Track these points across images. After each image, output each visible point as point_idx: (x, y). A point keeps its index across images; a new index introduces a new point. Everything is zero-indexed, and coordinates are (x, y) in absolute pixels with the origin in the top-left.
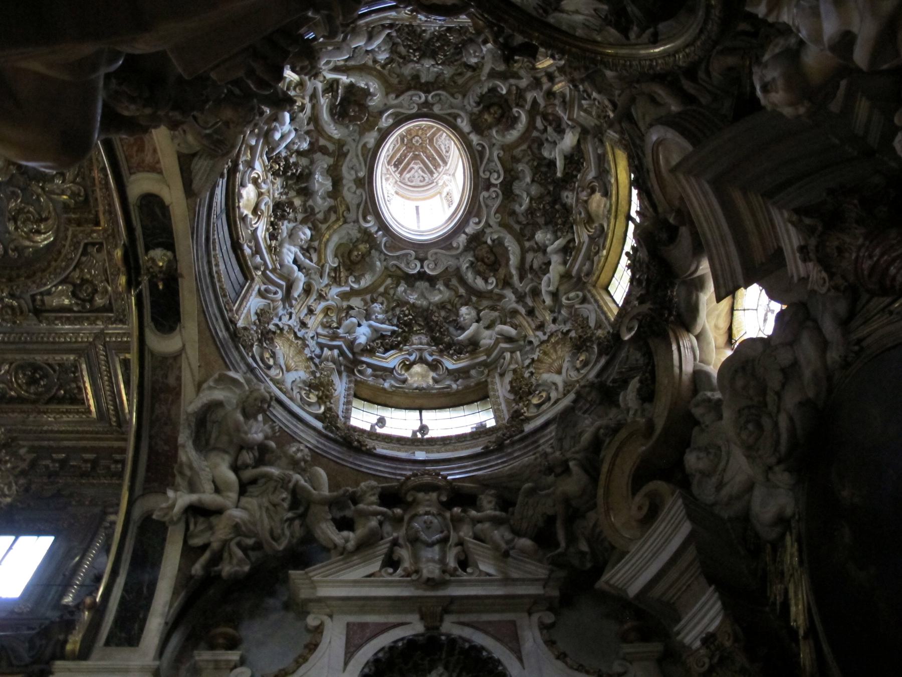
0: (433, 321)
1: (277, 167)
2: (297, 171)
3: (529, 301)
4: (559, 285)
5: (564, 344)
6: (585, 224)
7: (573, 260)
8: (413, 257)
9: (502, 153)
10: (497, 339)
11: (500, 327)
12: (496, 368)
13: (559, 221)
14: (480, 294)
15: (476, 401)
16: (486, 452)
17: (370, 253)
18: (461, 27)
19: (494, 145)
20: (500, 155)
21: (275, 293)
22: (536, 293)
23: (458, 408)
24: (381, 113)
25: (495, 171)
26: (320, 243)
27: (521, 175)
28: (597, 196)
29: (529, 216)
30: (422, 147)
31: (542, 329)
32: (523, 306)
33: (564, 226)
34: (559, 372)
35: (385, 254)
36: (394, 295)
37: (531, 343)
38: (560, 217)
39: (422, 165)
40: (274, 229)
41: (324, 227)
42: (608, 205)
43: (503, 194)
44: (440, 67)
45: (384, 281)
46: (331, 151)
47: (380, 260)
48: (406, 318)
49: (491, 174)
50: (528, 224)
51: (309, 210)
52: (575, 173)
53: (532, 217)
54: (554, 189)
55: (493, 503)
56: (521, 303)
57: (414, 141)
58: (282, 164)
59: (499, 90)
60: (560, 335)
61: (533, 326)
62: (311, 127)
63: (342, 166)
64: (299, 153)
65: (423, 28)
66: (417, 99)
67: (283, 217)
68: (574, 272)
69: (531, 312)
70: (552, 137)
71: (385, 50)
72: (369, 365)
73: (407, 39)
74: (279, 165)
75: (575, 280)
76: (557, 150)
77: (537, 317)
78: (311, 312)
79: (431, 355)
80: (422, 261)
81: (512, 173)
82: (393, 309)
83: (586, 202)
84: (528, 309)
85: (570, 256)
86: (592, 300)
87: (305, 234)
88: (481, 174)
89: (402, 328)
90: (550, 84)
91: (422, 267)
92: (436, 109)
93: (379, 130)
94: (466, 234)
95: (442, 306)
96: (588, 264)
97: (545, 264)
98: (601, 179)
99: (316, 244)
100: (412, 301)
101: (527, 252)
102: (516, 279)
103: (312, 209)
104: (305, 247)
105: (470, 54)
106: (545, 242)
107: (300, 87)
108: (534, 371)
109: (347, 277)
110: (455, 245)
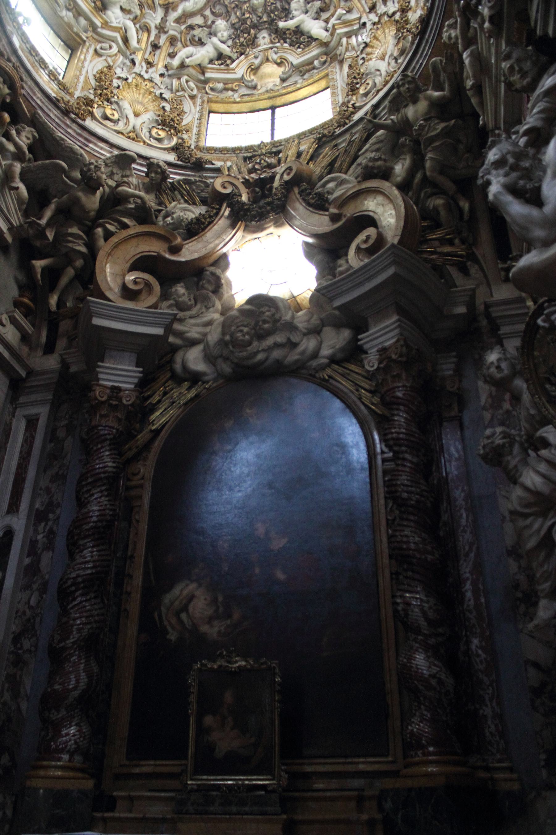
3: (163, 39)
4: (192, 66)
5: (154, 101)
6: (250, 67)
7: (217, 69)
10: (121, 28)
11: (130, 24)
12: (100, 42)
13: (242, 40)
15: (62, 40)
16: (54, 102)
22: (173, 41)
28: (279, 71)
29: (233, 5)
31: (149, 66)
32: (156, 35)
33: (240, 46)
34: (137, 115)
37: (133, 62)
38: (245, 38)
42: (277, 88)
50: (226, 6)
52: (288, 40)
53: (234, 8)
54: (266, 22)
55: (29, 142)
56: (157, 31)
60: (158, 93)
61: (146, 56)
68: (208, 75)
69: (155, 47)
70: (311, 7)
75: (203, 78)
76: (303, 17)
77: (154, 55)
83: (268, 60)
84: (156, 42)
85: (219, 65)
86: (198, 108)
96: (220, 86)
97: (200, 39)
98: (293, 71)
101: (202, 15)
102: (174, 15)
106: (218, 32)
108: (121, 88)
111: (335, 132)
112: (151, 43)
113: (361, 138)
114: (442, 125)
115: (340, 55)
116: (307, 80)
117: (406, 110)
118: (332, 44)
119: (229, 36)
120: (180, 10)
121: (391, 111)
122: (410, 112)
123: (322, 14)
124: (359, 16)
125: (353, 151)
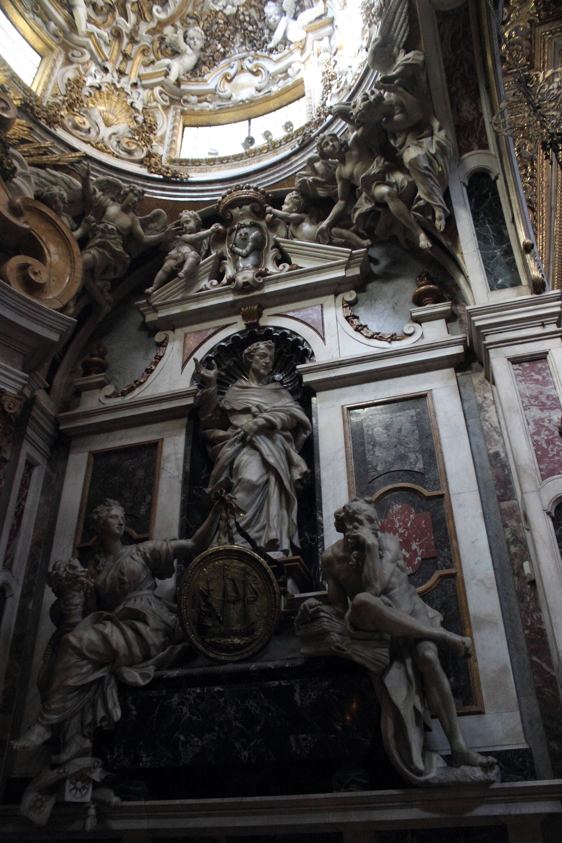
18: (215, 65)
44: (218, 9)
59: (160, 9)
65: (244, 48)
71: (270, 18)
73: (254, 33)
90: (123, 48)
105: (198, 39)
111: (40, 119)
113: (58, 161)
114: (120, 249)
115: (73, 55)
116: (36, 24)
117: (111, 202)
118: (75, 37)
121: (99, 183)
122: (113, 209)
123: (91, 7)
124: (108, 57)
125: (45, 158)
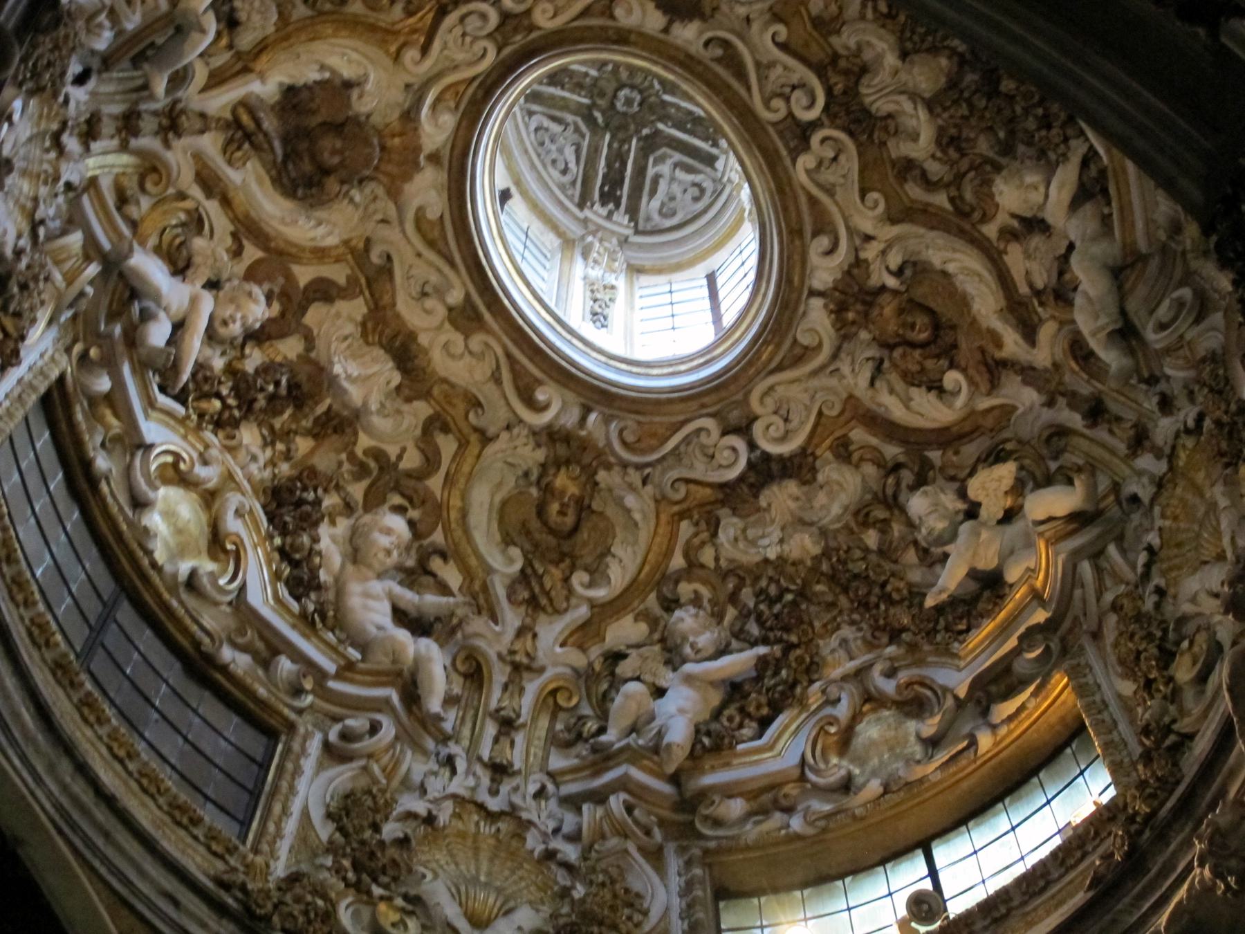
0: (856, 576)
1: (217, 404)
2: (277, 384)
8: (715, 433)
9: (782, 30)
14: (947, 438)
17: (596, 484)
19: (748, 20)
20: (782, 37)
21: (374, 728)
23: (1026, 788)
24: (410, 116)
25: (794, 88)
26: (447, 531)
27: (867, 55)
29: (953, 153)
30: (652, 109)
32: (1072, 406)
35: (639, 467)
36: (717, 559)
38: (1026, 111)
39: (678, 157)
40: (295, 564)
41: (435, 483)
43: (851, 134)
45: (673, 536)
46: (342, 281)
47: (631, 488)
48: (777, 608)
49: (787, 99)
51: (372, 464)
57: (619, 105)
58: (225, 392)
61: (1122, 448)
62: (252, 253)
63: (394, 305)
64: (258, 336)
66: (478, 23)
67: (310, 521)
72: (728, 791)
74: (218, 395)
77: (1118, 419)
78: (507, 725)
79: (890, 674)
80: (744, 429)
81: (843, 64)
82: (734, 598)
84: (1086, 407)
87: (388, 531)
88: (766, 115)
89: (779, 641)
91: (752, 446)
92: (544, 19)
93: (434, 158)
94: (821, 294)
95: (862, 516)
99: (438, 537)
100: (772, 554)
102: (1012, 343)
103: (377, 454)
104: (411, 563)
107: (155, 176)
109: (566, 580)
110: (805, 340)
112: (1087, 427)
119: (1039, 159)
120: (997, 325)
